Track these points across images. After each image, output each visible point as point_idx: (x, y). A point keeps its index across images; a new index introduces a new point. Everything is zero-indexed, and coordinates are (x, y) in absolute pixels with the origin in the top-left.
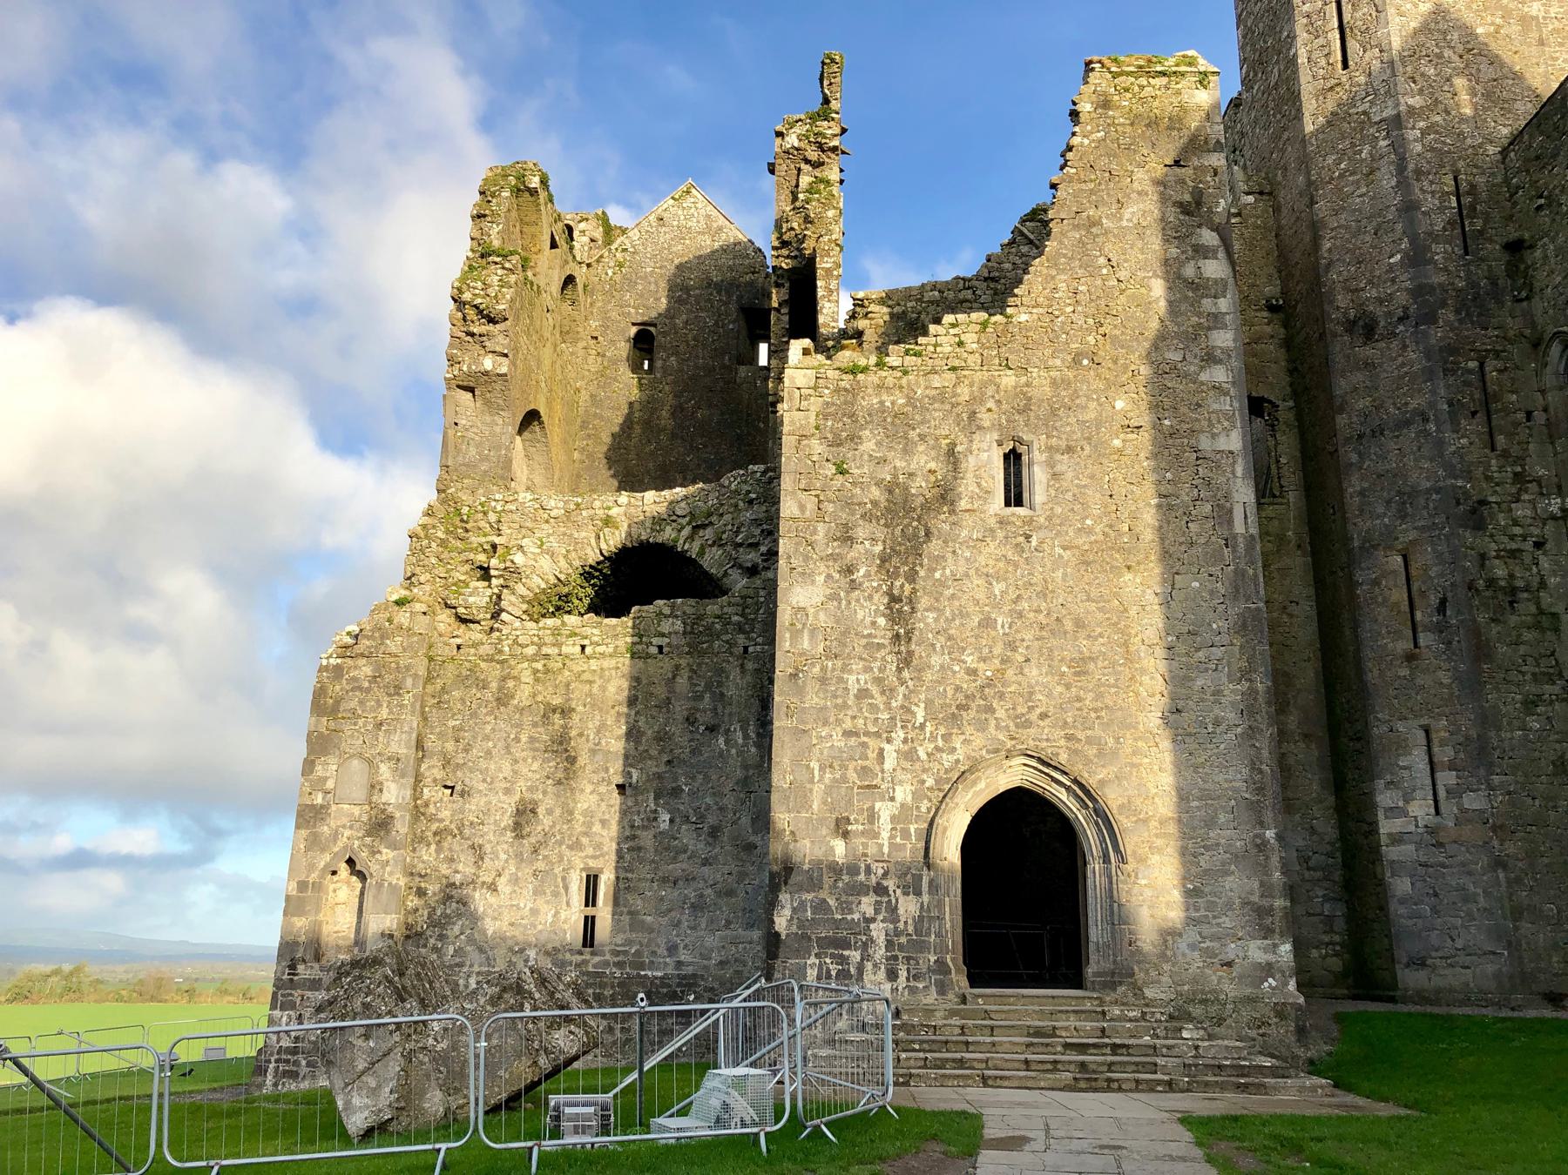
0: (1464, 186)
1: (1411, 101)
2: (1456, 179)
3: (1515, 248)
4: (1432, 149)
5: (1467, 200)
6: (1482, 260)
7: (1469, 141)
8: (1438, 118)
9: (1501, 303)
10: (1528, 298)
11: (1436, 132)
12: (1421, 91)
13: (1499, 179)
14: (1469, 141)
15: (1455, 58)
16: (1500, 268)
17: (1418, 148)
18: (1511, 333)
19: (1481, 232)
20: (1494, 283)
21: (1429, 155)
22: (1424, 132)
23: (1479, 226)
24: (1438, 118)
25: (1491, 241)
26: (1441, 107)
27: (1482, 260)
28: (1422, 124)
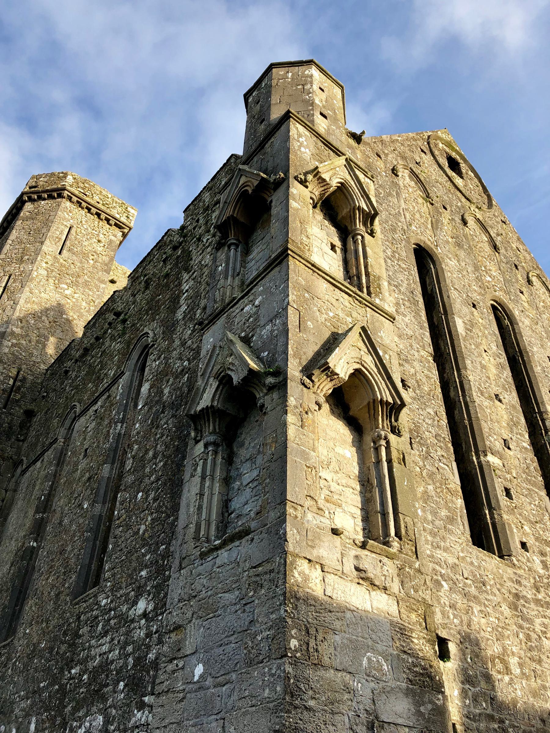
0: (20, 376)
1: (14, 329)
2: (18, 372)
3: (30, 414)
4: (13, 354)
5: (18, 383)
6: (11, 414)
7: (34, 358)
8: (24, 342)
9: (9, 438)
10: (23, 441)
11: (19, 348)
12: (22, 328)
13: (39, 381)
14: (34, 358)
15: (47, 322)
16: (17, 422)
17: (7, 350)
18: (6, 455)
19: (17, 401)
20: (10, 428)
21: (10, 356)
22: (13, 345)
23: (18, 397)
24: (24, 342)
25: (20, 407)
26: (28, 338)
27: (11, 414)
28: (14, 341)
